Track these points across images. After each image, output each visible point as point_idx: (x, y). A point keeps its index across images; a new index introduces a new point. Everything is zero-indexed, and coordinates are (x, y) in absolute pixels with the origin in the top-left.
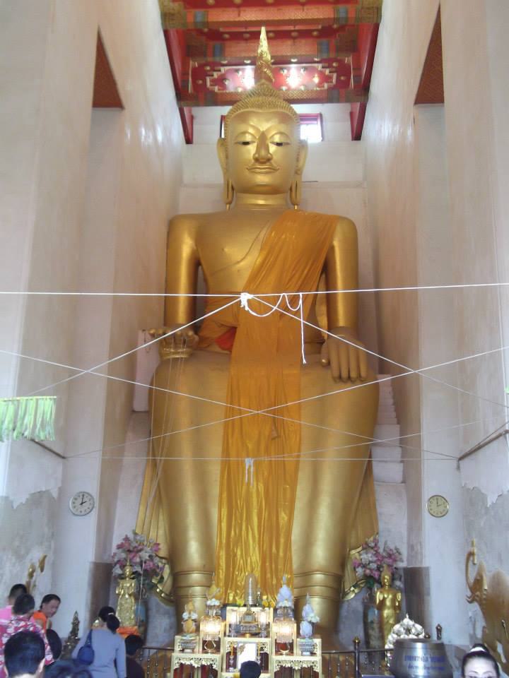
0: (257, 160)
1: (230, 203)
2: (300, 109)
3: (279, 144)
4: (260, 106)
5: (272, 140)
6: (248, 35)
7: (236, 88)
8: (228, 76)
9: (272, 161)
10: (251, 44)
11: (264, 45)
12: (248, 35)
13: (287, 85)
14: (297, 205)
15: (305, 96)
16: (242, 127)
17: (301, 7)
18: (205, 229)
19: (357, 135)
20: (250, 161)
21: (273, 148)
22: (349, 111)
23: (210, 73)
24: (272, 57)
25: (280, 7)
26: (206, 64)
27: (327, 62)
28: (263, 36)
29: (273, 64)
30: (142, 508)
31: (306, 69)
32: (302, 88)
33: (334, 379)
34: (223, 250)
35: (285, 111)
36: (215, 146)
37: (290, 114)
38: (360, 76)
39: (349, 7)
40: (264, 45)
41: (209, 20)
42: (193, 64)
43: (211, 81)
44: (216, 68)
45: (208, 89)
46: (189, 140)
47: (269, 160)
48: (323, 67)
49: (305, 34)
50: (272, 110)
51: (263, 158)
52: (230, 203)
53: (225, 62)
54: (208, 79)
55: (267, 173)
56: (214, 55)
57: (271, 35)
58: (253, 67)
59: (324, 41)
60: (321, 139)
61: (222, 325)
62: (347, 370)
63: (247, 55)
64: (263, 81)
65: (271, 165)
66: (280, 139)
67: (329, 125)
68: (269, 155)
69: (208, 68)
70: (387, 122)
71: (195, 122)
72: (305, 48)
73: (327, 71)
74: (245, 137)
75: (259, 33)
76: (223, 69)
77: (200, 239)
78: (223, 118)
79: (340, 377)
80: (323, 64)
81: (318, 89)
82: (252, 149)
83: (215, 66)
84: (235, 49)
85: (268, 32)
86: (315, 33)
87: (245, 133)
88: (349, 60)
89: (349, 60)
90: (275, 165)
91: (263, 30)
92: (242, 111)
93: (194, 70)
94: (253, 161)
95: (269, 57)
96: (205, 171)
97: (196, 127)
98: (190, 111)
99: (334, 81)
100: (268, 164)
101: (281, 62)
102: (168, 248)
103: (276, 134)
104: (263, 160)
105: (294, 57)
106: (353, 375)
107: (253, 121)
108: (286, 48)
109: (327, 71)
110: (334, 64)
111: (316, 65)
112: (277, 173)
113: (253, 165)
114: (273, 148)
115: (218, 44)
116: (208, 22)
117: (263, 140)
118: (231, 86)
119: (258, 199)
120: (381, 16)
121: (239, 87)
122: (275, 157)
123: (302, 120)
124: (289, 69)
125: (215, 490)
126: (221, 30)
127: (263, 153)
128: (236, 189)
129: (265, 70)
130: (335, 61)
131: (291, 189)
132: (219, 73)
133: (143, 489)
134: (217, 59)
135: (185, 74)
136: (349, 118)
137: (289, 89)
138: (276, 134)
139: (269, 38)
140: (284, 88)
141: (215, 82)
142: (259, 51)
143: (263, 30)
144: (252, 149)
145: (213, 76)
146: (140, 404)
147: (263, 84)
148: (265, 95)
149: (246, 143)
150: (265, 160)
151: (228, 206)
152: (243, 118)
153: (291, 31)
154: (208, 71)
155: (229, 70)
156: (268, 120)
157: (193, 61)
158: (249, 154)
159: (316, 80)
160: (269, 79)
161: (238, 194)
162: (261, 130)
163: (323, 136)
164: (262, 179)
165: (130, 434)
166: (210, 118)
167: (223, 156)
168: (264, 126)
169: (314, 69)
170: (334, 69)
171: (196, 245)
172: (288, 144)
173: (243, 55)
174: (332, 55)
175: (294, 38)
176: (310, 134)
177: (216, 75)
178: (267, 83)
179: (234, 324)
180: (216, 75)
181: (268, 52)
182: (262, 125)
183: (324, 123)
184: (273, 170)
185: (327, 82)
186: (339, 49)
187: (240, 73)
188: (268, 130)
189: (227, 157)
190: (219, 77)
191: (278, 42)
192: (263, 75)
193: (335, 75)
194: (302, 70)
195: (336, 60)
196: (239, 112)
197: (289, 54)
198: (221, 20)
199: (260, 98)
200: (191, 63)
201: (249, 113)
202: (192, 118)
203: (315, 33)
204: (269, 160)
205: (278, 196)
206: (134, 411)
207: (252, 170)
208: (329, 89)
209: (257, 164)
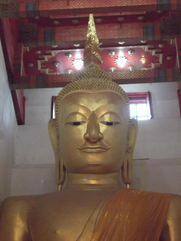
0: (88, 140)
1: (62, 184)
2: (128, 88)
3: (109, 124)
4: (90, 87)
5: (101, 120)
6: (76, 21)
7: (66, 70)
8: (59, 59)
9: (103, 141)
11: (92, 30)
12: (76, 21)
13: (116, 66)
14: (130, 184)
15: (133, 76)
16: (73, 108)
21: (103, 128)
22: (177, 89)
23: (42, 57)
24: (100, 41)
26: (38, 49)
27: (153, 44)
28: (91, 22)
29: (101, 47)
31: (132, 50)
32: (130, 69)
34: (55, 232)
35: (114, 91)
36: (47, 127)
37: (119, 94)
40: (92, 30)
41: (40, 9)
42: (26, 48)
43: (42, 64)
44: (47, 52)
45: (39, 71)
46: (20, 121)
47: (100, 139)
48: (149, 49)
50: (101, 91)
51: (94, 139)
52: (62, 184)
53: (56, 46)
54: (39, 63)
55: (97, 153)
57: (99, 20)
58: (83, 50)
60: (151, 116)
63: (76, 39)
64: (92, 63)
65: (102, 144)
66: (110, 118)
67: (157, 103)
69: (39, 52)
71: (26, 103)
72: (131, 31)
73: (153, 53)
74: (76, 118)
75: (87, 19)
76: (54, 53)
78: (54, 99)
80: (149, 46)
81: (146, 69)
82: (83, 129)
83: (46, 50)
85: (95, 18)
86: (140, 18)
90: (105, 143)
91: (91, 16)
92: (72, 92)
93: (26, 54)
94: (84, 141)
95: (97, 41)
96: (37, 150)
97: (27, 108)
98: (22, 93)
99: (161, 61)
100: (99, 143)
101: (109, 45)
103: (106, 113)
104: (93, 140)
105: (121, 40)
107: (84, 102)
108: (113, 33)
109: (153, 53)
110: (160, 46)
111: (142, 47)
112: (109, 151)
113: (84, 145)
114: (103, 128)
117: (93, 119)
118: (61, 68)
119: (89, 179)
121: (69, 69)
122: (105, 137)
123: (131, 99)
124: (116, 51)
126: (51, 17)
127: (94, 132)
128: (68, 168)
129: (94, 53)
130: (160, 43)
131: (122, 168)
132: (50, 57)
134: (48, 44)
135: (17, 58)
136: (176, 95)
137: (117, 70)
138: (106, 113)
139: (97, 24)
140: (113, 69)
141: (46, 65)
142: (88, 35)
143: (91, 16)
144: (83, 129)
145: (44, 59)
147: (92, 66)
148: (94, 76)
149: (78, 124)
150: (95, 140)
151: (60, 186)
152: (74, 99)
153: (116, 17)
154: (41, 54)
155: (60, 53)
156: (98, 101)
157: (24, 46)
158: (80, 133)
159: (143, 61)
160: (98, 62)
162: (92, 110)
163: (152, 114)
164: (93, 158)
167: (54, 136)
168: (94, 107)
170: (160, 51)
171: (28, 228)
172: (118, 123)
173: (72, 39)
174: (158, 38)
175: (121, 23)
176: (140, 112)
177: (46, 58)
178: (96, 65)
180: (46, 58)
181: (96, 36)
182: (92, 105)
183: (153, 102)
184: (103, 149)
185: (154, 62)
187: (70, 56)
188: (98, 110)
189: (58, 137)
190: (49, 60)
192: (92, 57)
193: (161, 56)
194: (129, 53)
195: (161, 42)
196: (69, 93)
197: (116, 37)
198: (51, 9)
199: (90, 80)
200: (23, 47)
201: (79, 94)
202: (24, 99)
204: (100, 139)
205: (109, 175)
207: (83, 150)
208: (157, 68)
209: (88, 144)
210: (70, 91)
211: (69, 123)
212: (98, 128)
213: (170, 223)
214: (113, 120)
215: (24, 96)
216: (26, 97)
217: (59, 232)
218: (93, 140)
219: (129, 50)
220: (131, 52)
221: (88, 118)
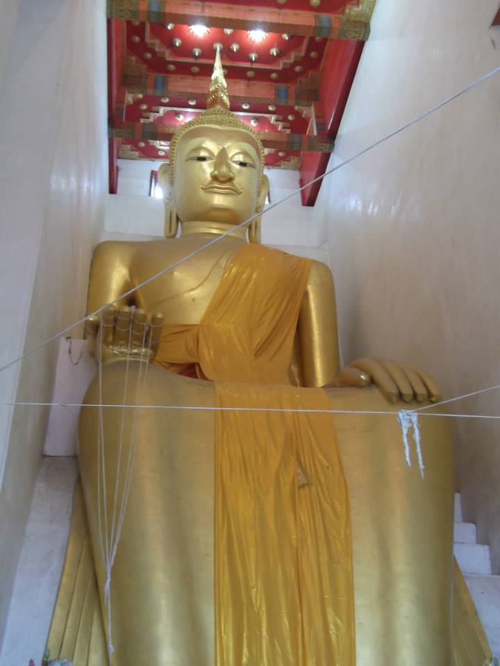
3: (242, 164)
6: (196, 69)
9: (235, 182)
10: (200, 82)
11: (218, 73)
12: (196, 69)
16: (195, 142)
17: (277, 10)
18: (143, 257)
19: (310, 201)
20: (206, 179)
22: (298, 179)
25: (253, 8)
27: (282, 112)
30: (59, 611)
31: (257, 119)
33: (389, 398)
34: (172, 273)
38: (326, 124)
39: (332, 16)
40: (218, 73)
42: (129, 98)
46: (113, 190)
48: (277, 120)
49: (262, 75)
50: (232, 129)
51: (224, 176)
53: (166, 101)
56: (155, 87)
59: (282, 86)
61: (173, 365)
62: (409, 386)
64: (218, 107)
65: (233, 185)
68: (231, 174)
69: (145, 107)
70: (350, 186)
71: (120, 173)
72: (261, 91)
76: (162, 110)
77: (137, 269)
79: (401, 396)
83: (154, 102)
84: (181, 85)
85: (224, 67)
86: (274, 76)
87: (199, 148)
88: (310, 112)
89: (310, 112)
90: (237, 186)
92: (196, 126)
93: (129, 107)
94: (210, 178)
102: (91, 277)
105: (245, 100)
106: (420, 390)
108: (241, 88)
110: (290, 118)
112: (241, 196)
113: (211, 183)
115: (160, 76)
116: (164, 13)
120: (369, 31)
125: (206, 573)
127: (224, 169)
129: (222, 95)
131: (250, 227)
133: (62, 575)
134: (158, 93)
142: (213, 77)
144: (207, 168)
146: (58, 444)
149: (203, 159)
158: (204, 171)
161: (186, 224)
164: (218, 200)
165: (41, 486)
166: (137, 171)
169: (267, 120)
171: (131, 278)
173: (190, 90)
174: (291, 102)
177: (152, 117)
179: (192, 360)
184: (235, 192)
186: (299, 97)
191: (233, 80)
192: (219, 100)
193: (288, 131)
197: (242, 95)
198: (181, 13)
202: (118, 169)
203: (274, 76)
204: (230, 180)
206: (44, 456)
207: (208, 189)
210: (193, 125)
211: (192, 159)
212: (229, 167)
213: (310, 288)
214: (248, 161)
215: (118, 165)
216: (120, 167)
217: (176, 274)
218: (222, 179)
219: (254, 119)
220: (255, 122)
221: (216, 154)
